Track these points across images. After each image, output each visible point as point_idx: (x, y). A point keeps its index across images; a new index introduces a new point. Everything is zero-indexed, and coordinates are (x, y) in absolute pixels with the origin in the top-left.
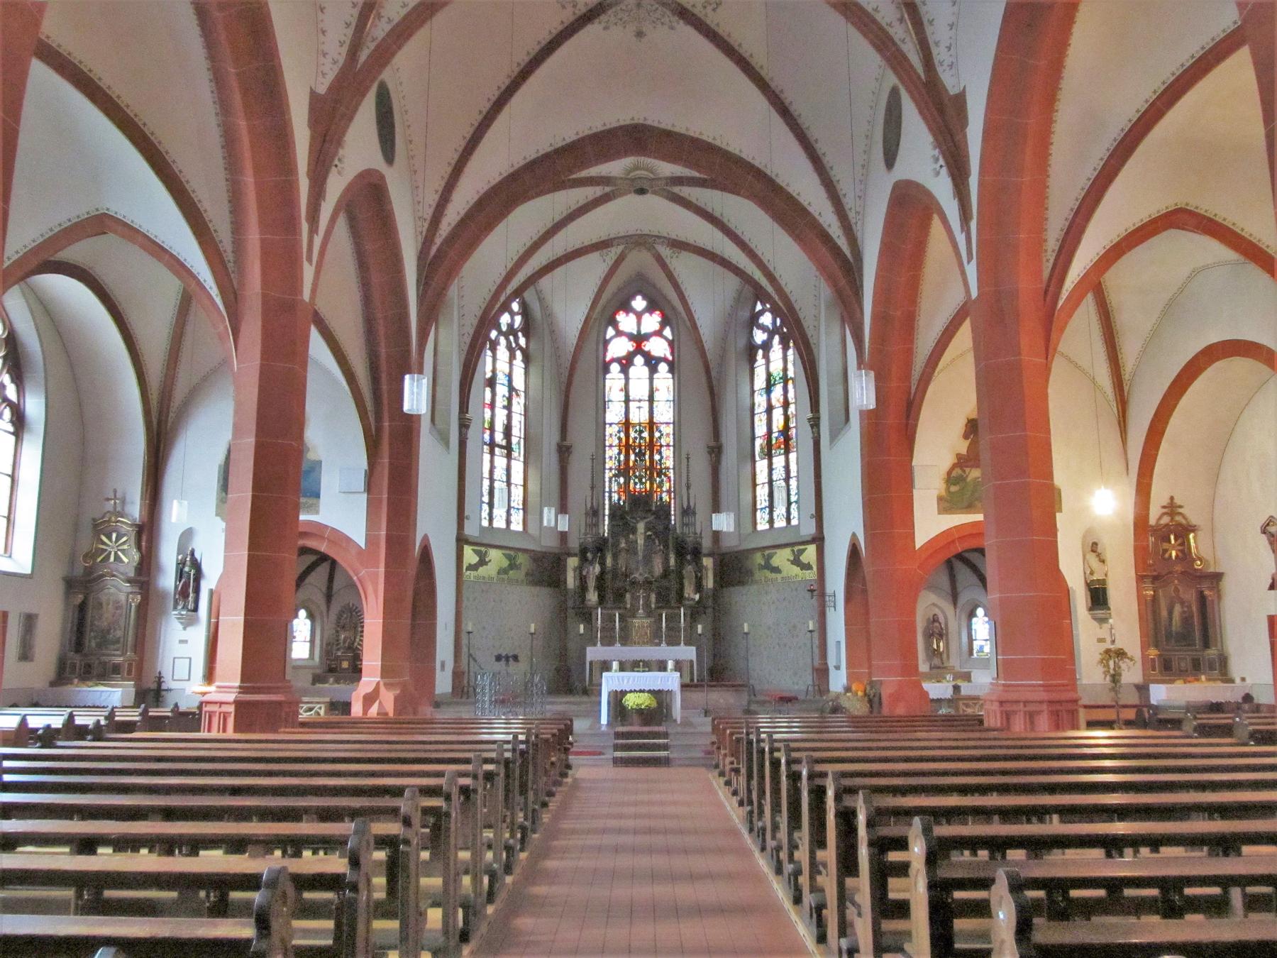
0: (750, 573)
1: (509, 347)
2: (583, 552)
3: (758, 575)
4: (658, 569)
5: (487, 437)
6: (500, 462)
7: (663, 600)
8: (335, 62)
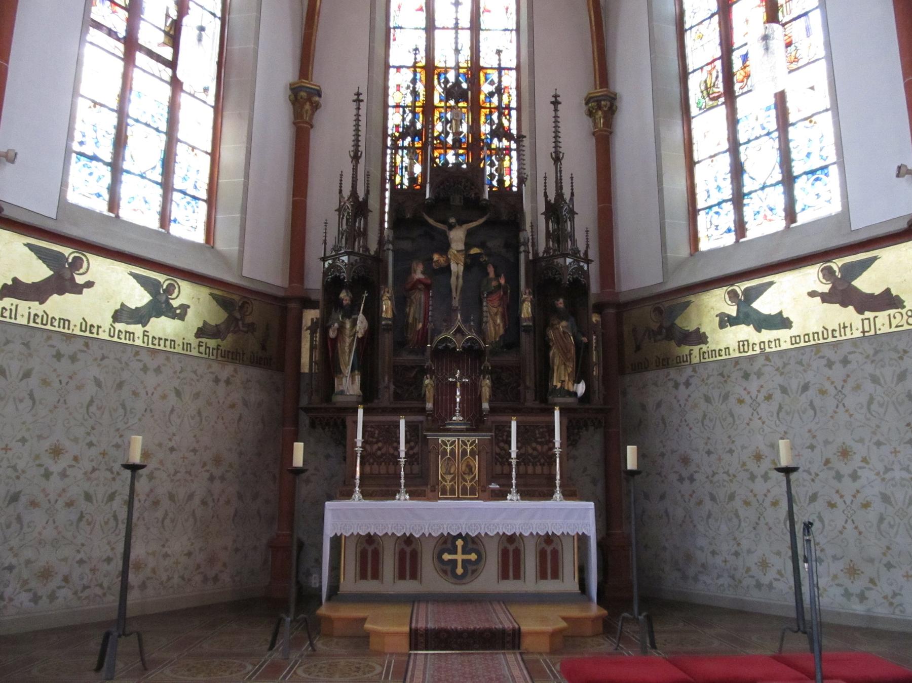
2: (333, 284)
4: (495, 326)
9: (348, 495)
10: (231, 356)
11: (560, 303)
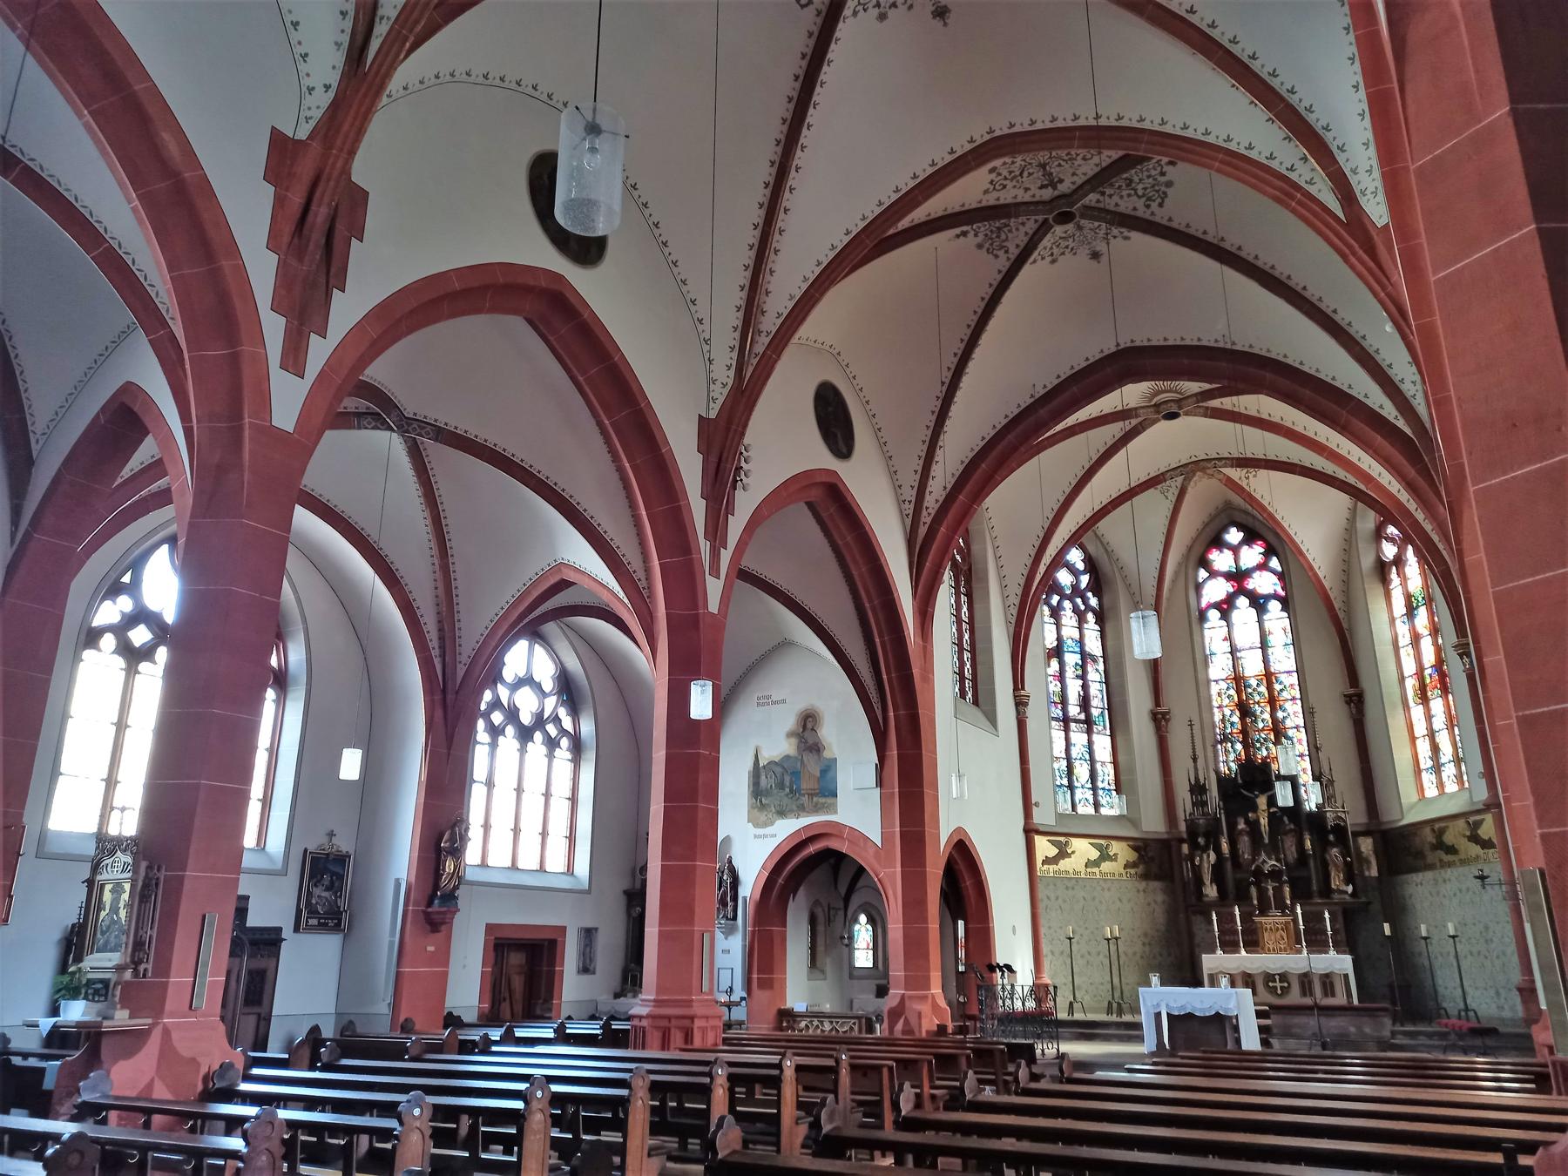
0: (1420, 854)
1: (1076, 610)
3: (1431, 857)
4: (1291, 852)
5: (1058, 712)
6: (1079, 738)
7: (1301, 894)
8: (724, 385)
9: (1214, 952)
10: (1146, 876)
11: (1331, 837)
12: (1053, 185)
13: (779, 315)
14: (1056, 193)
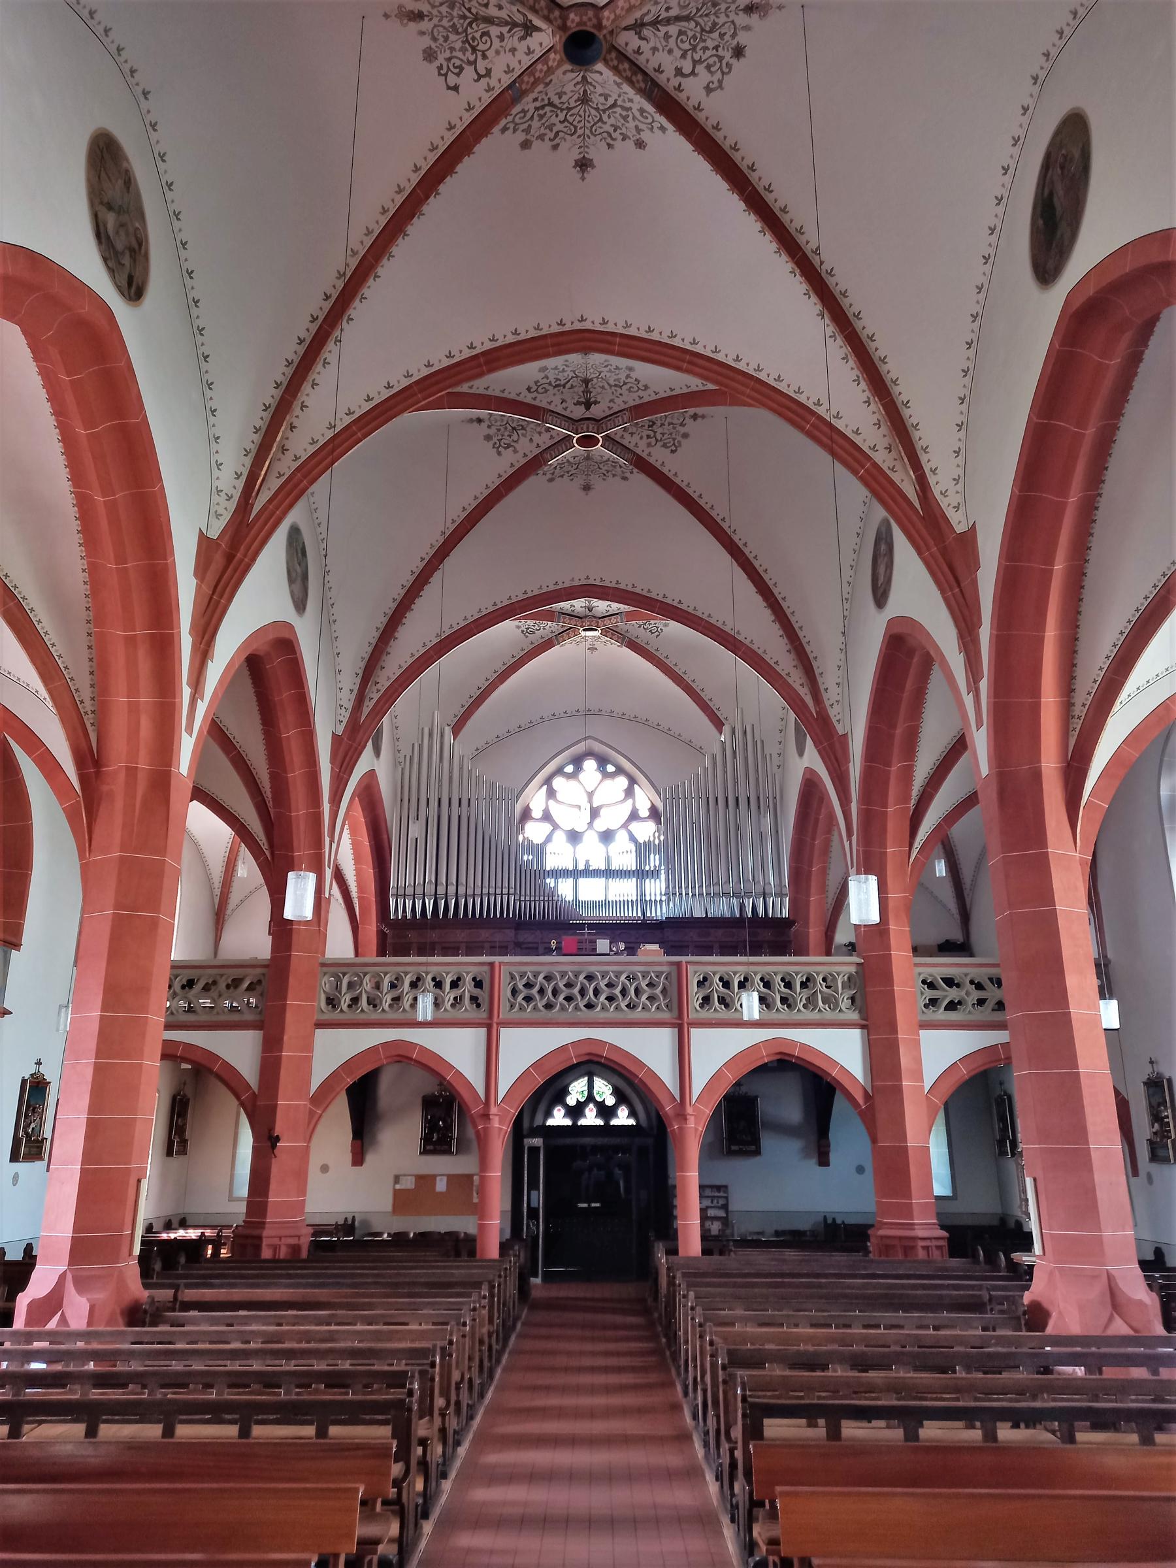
12: (588, 405)
13: (314, 442)
14: (588, 415)
